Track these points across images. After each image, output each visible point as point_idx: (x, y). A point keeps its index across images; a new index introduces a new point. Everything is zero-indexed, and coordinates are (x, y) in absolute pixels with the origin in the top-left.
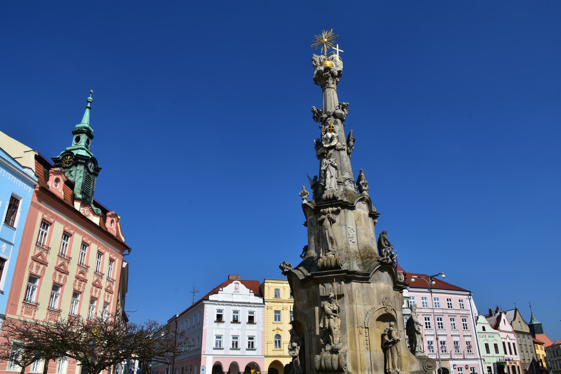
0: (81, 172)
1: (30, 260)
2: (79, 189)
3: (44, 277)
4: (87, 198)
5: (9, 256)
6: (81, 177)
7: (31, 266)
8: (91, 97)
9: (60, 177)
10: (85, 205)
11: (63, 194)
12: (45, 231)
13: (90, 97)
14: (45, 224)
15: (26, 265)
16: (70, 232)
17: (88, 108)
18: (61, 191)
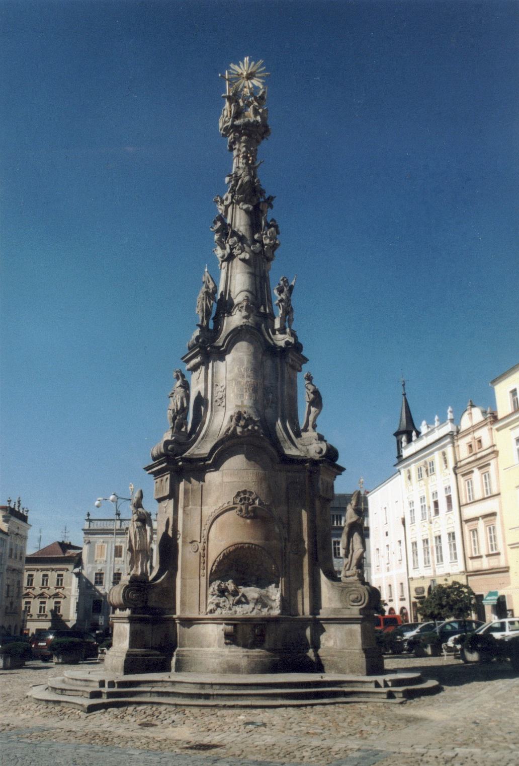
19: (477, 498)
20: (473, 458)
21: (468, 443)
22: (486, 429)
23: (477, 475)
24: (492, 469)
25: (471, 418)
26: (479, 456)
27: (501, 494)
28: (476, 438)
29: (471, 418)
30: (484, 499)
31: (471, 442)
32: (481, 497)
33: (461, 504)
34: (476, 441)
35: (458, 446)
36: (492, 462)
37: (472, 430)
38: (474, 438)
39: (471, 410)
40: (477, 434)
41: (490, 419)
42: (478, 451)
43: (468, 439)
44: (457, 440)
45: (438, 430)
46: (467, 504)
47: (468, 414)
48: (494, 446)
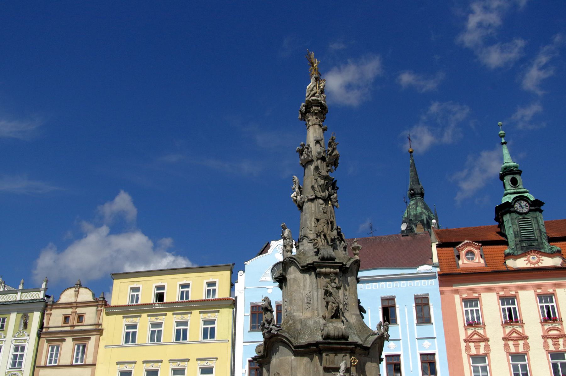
0: (508, 222)
1: (463, 345)
2: (513, 241)
3: (491, 354)
4: (531, 243)
5: (435, 349)
6: (510, 227)
7: (468, 348)
8: (502, 130)
9: (463, 252)
10: (530, 253)
11: (482, 261)
12: (474, 309)
13: (500, 131)
14: (471, 302)
15: (460, 350)
16: (511, 294)
17: (505, 143)
18: (479, 260)
19: (62, 362)
20: (68, 329)
21: (64, 315)
22: (94, 309)
23: (68, 345)
24: (91, 344)
25: (77, 296)
26: (76, 328)
27: (97, 365)
28: (77, 313)
29: (77, 296)
30: (72, 366)
31: (70, 315)
32: (68, 363)
33: (37, 365)
34: (77, 316)
35: (51, 314)
36: (93, 338)
37: (75, 305)
38: (76, 312)
39: (79, 289)
40: (80, 311)
41: (102, 302)
42: (75, 323)
43: (68, 311)
44: (51, 309)
45: (22, 293)
46: (45, 367)
47: (75, 291)
48: (101, 325)
